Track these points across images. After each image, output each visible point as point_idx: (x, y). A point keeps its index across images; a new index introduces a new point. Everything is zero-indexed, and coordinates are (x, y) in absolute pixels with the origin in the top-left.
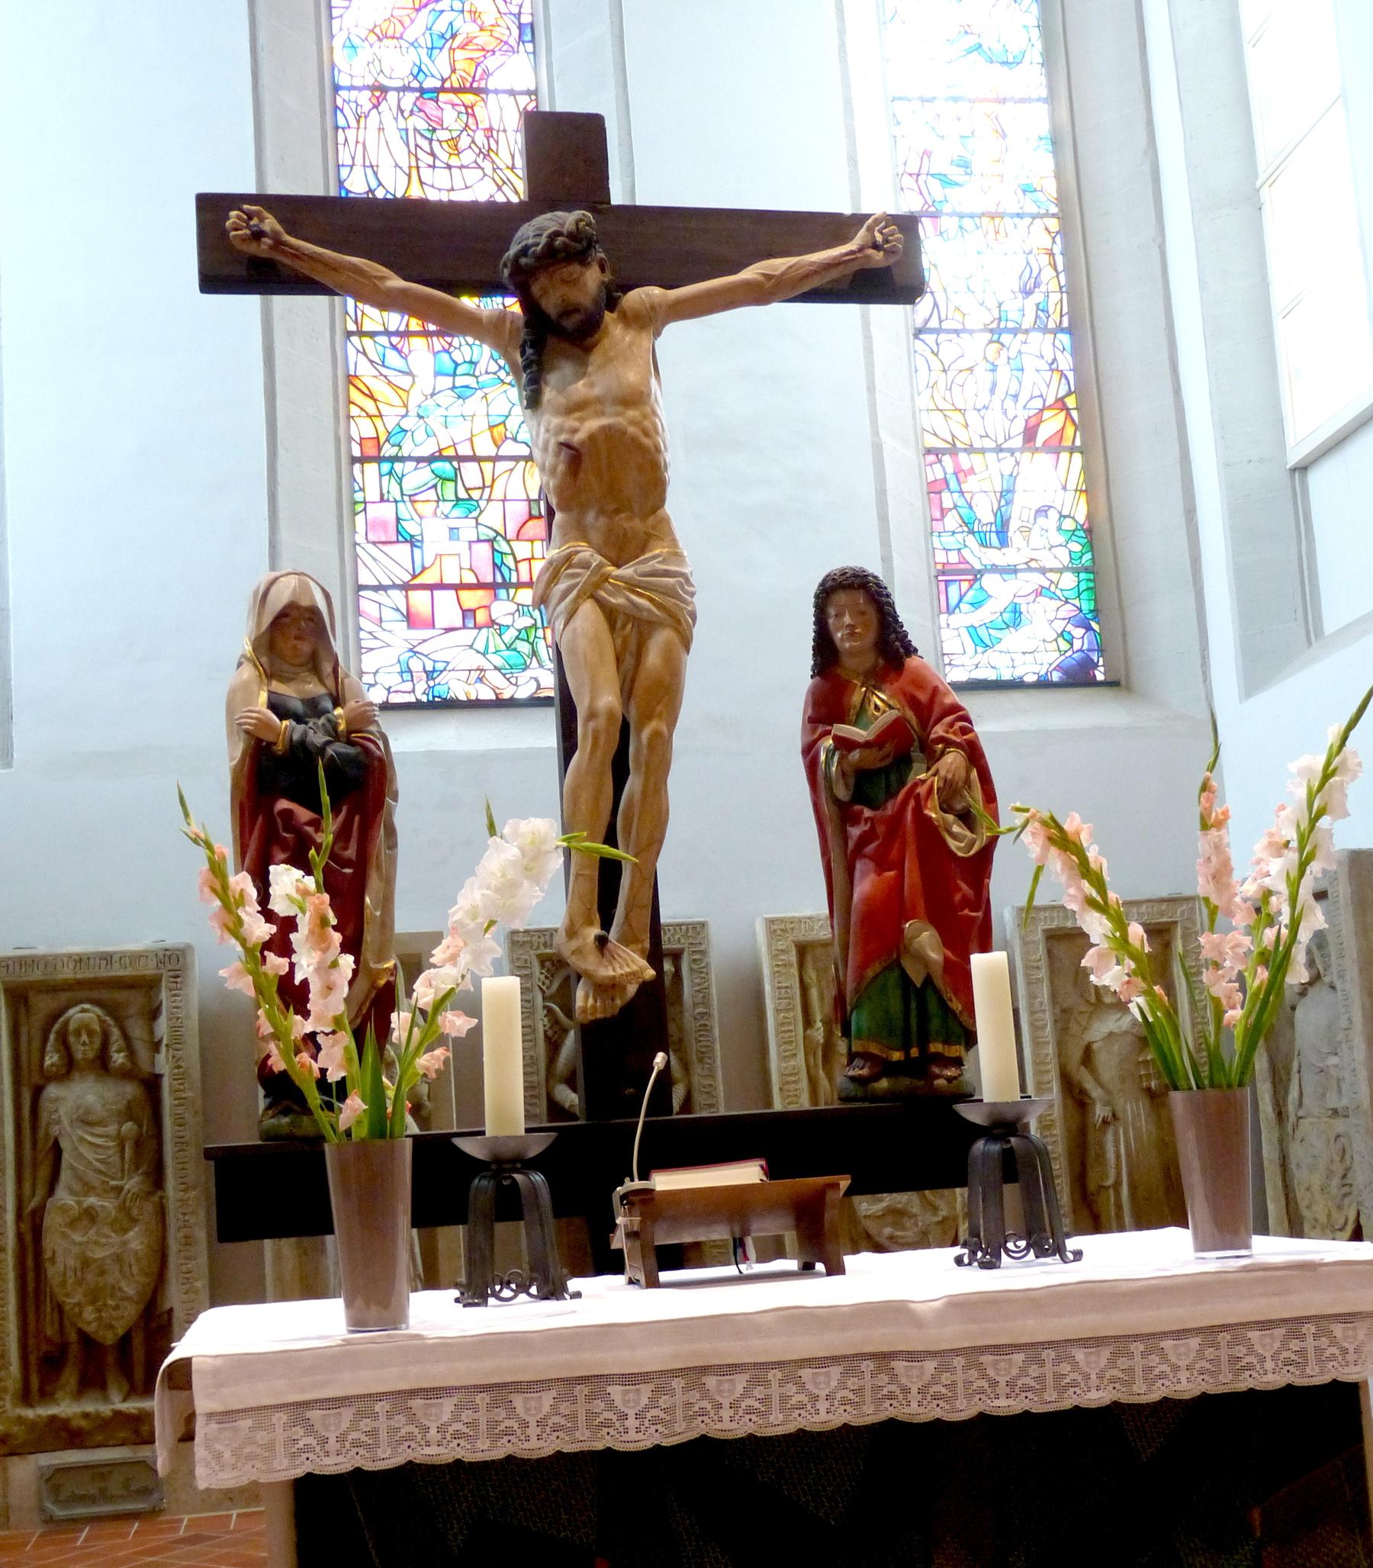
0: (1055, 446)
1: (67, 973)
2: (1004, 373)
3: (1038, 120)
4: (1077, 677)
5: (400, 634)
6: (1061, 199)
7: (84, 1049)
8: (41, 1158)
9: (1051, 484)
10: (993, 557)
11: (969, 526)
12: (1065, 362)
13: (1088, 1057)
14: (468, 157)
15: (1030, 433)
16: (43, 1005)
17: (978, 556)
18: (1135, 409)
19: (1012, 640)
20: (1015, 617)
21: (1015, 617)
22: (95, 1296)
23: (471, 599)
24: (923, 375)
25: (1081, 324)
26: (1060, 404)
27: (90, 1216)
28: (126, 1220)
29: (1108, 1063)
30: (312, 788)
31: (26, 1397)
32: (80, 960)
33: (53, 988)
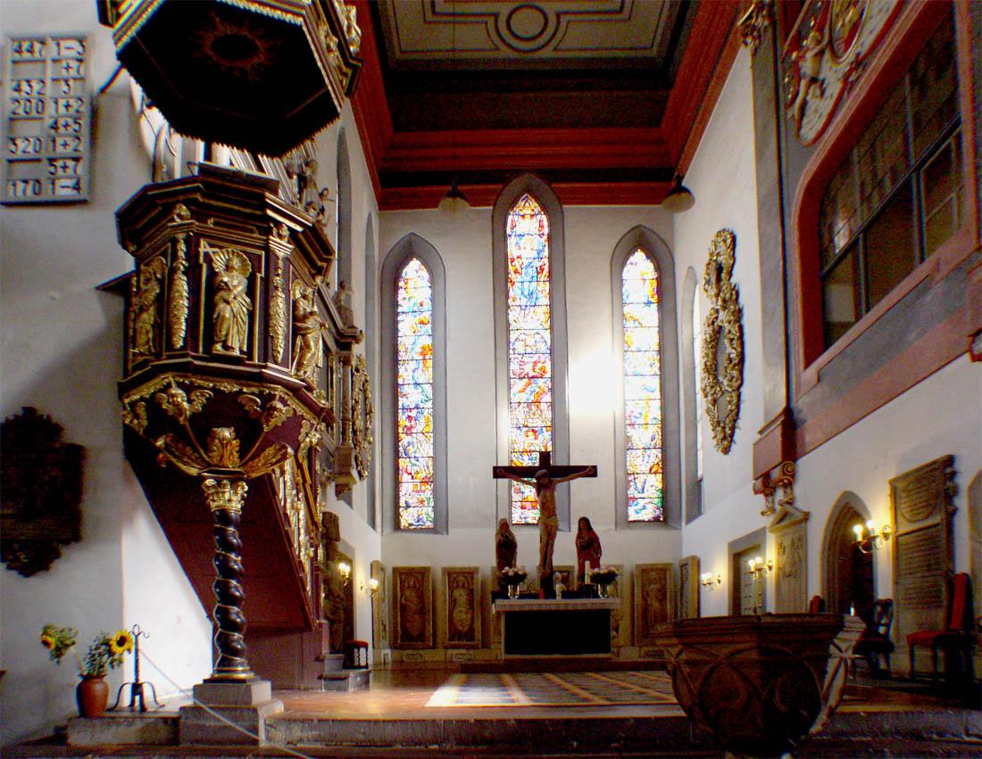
0: (655, 473)
1: (458, 570)
2: (646, 457)
3: (657, 404)
4: (656, 519)
5: (520, 510)
6: (661, 421)
7: (461, 584)
8: (453, 602)
9: (655, 482)
10: (642, 496)
11: (636, 489)
12: (660, 455)
13: (647, 593)
14: (537, 416)
15: (651, 470)
16: (455, 575)
17: (637, 495)
18: (672, 467)
19: (643, 512)
20: (644, 508)
21: (644, 508)
22: (461, 625)
23: (534, 504)
24: (628, 459)
25: (664, 448)
26: (658, 464)
27: (461, 611)
28: (467, 613)
29: (652, 594)
30: (506, 547)
31: (450, 640)
32: (460, 568)
33: (455, 573)
